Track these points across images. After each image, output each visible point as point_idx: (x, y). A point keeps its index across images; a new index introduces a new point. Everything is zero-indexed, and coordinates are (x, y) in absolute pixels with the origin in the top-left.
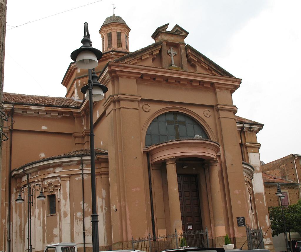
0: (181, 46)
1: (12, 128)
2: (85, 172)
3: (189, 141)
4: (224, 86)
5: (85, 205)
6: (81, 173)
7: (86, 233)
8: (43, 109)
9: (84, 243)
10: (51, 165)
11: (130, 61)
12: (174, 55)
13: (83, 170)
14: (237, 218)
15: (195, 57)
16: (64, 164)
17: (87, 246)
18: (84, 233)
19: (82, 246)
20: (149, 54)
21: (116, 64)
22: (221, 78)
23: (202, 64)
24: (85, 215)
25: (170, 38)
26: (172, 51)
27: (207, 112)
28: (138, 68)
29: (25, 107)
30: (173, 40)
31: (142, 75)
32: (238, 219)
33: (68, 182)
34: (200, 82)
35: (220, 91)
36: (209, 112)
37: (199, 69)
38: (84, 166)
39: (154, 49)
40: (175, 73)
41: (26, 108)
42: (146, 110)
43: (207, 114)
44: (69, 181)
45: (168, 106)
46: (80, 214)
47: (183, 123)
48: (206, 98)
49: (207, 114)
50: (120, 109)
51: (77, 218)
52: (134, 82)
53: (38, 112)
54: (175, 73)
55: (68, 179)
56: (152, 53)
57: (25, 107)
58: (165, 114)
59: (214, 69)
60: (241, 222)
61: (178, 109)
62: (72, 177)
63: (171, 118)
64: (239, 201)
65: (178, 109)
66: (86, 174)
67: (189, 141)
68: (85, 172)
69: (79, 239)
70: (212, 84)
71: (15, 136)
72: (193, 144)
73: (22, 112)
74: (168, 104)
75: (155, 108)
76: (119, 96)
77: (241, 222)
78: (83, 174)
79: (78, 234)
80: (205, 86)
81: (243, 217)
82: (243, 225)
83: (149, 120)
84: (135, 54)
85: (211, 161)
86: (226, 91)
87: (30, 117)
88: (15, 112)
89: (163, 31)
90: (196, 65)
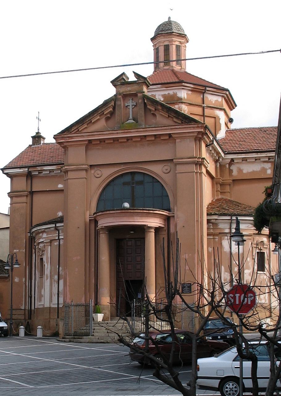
0: (139, 95)
1: (31, 189)
2: (61, 237)
6: (57, 238)
7: (60, 295)
8: (55, 168)
9: (58, 304)
10: (40, 231)
12: (134, 106)
13: (59, 235)
16: (46, 230)
18: (58, 294)
21: (60, 137)
24: (60, 278)
26: (130, 103)
27: (166, 167)
29: (39, 168)
30: (130, 91)
34: (155, 135)
35: (180, 142)
38: (60, 232)
39: (104, 109)
41: (40, 169)
42: (98, 176)
45: (122, 167)
46: (56, 277)
47: (141, 183)
51: (54, 281)
53: (50, 171)
56: (102, 113)
58: (122, 175)
60: (186, 288)
62: (53, 242)
66: (62, 240)
69: (55, 301)
70: (170, 135)
71: (36, 198)
73: (39, 173)
74: (122, 166)
75: (107, 173)
76: (66, 167)
77: (186, 288)
79: (55, 296)
83: (100, 185)
87: (46, 177)
88: (32, 174)
89: (117, 84)
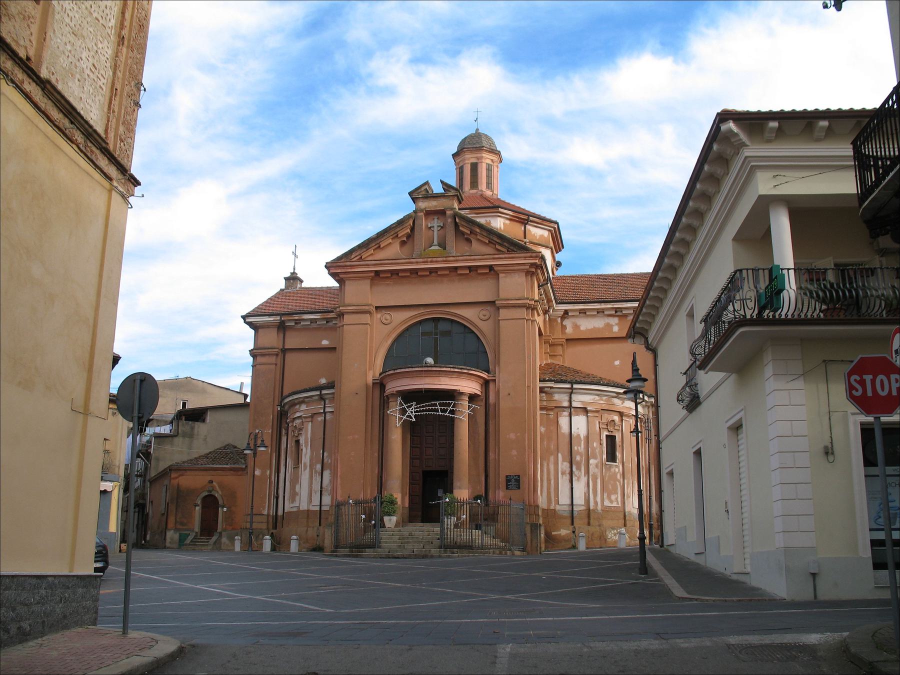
0: (449, 213)
1: (284, 346)
2: (327, 410)
3: (407, 370)
4: (511, 268)
5: (325, 454)
6: (322, 411)
7: (323, 492)
8: (319, 317)
9: (321, 505)
10: (296, 401)
11: (360, 254)
12: (440, 228)
13: (325, 407)
14: (507, 476)
15: (467, 227)
16: (306, 400)
17: (324, 508)
18: (321, 491)
19: (318, 508)
20: (391, 237)
21: (335, 265)
22: (501, 256)
23: (478, 237)
24: (324, 468)
25: (430, 204)
26: (436, 223)
27: (484, 312)
28: (368, 265)
29: (296, 317)
30: (436, 206)
31: (377, 273)
32: (508, 479)
33: (310, 423)
34: (469, 268)
35: (505, 277)
36: (486, 312)
37: (476, 245)
38: (327, 402)
39: (398, 229)
40: (423, 262)
41: (297, 318)
42: (386, 322)
43: (485, 316)
44: (310, 423)
45: (422, 310)
46: (319, 467)
47: (447, 333)
48: (479, 290)
49: (485, 316)
50: (343, 326)
51: (316, 472)
52: (365, 285)
53: (312, 321)
54: (423, 262)
55: (310, 419)
56: (396, 235)
57: (296, 317)
58: (420, 322)
59: (497, 241)
60: (513, 482)
61: (436, 313)
62: (315, 416)
63: (429, 327)
64: (513, 451)
65: (436, 313)
66: (329, 413)
67: (407, 370)
68: (327, 410)
69: (316, 500)
70: (491, 268)
71: (289, 357)
72: (423, 373)
73: (296, 323)
74: (422, 308)
75: (401, 319)
76: (341, 308)
77: (513, 482)
78: (325, 413)
79: (316, 493)
80: (479, 272)
81: (517, 475)
82: (515, 488)
83: (389, 335)
84: (367, 244)
85: (455, 394)
86: (516, 275)
87: (306, 328)
88: (286, 325)
89: (417, 196)
90: (471, 239)
